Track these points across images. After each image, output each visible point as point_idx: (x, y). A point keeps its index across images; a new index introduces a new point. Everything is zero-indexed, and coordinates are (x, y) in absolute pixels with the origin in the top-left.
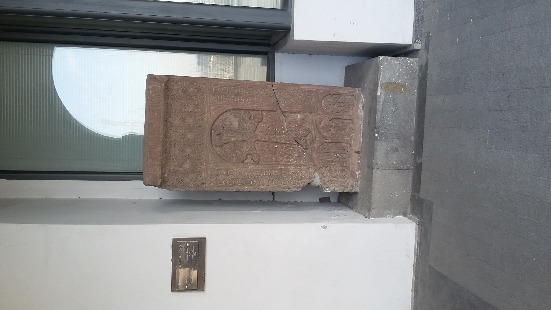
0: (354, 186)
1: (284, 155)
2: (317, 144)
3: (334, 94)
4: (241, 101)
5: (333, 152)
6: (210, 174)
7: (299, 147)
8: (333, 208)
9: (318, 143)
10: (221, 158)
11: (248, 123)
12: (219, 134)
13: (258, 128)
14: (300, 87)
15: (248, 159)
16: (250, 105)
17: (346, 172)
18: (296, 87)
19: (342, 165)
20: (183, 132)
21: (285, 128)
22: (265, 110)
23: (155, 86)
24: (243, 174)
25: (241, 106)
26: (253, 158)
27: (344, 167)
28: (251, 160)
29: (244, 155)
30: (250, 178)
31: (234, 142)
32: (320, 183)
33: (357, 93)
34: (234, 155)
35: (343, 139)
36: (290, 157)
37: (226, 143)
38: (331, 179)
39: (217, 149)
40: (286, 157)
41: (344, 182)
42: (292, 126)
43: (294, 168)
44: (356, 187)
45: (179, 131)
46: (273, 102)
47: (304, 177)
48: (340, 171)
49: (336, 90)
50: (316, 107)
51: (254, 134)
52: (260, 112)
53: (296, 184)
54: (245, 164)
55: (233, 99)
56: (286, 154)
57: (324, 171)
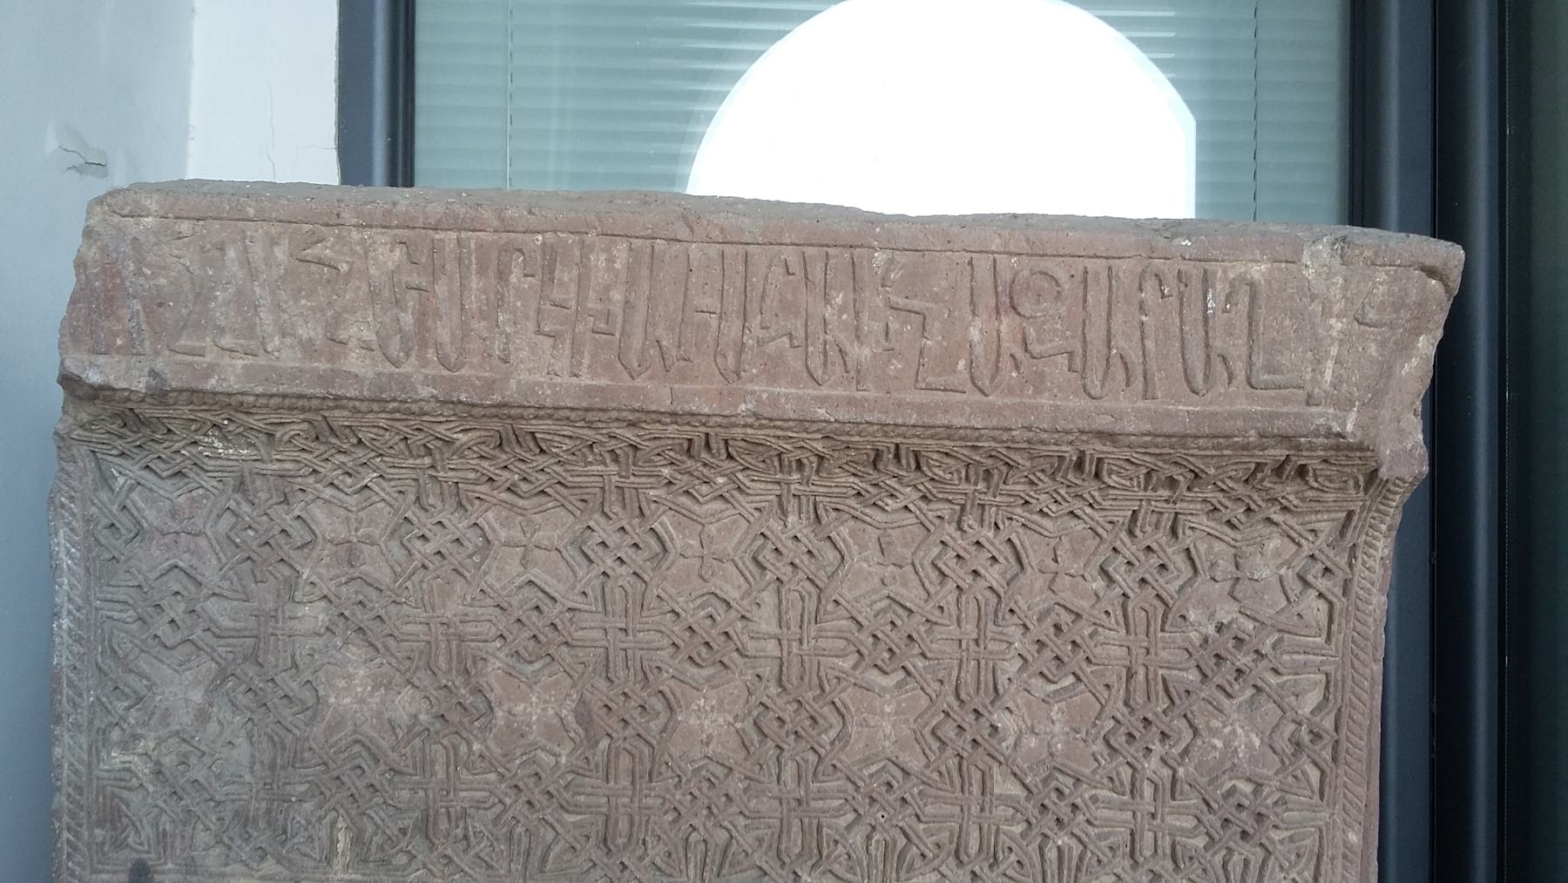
20: (751, 647)
23: (1337, 325)
45: (768, 597)
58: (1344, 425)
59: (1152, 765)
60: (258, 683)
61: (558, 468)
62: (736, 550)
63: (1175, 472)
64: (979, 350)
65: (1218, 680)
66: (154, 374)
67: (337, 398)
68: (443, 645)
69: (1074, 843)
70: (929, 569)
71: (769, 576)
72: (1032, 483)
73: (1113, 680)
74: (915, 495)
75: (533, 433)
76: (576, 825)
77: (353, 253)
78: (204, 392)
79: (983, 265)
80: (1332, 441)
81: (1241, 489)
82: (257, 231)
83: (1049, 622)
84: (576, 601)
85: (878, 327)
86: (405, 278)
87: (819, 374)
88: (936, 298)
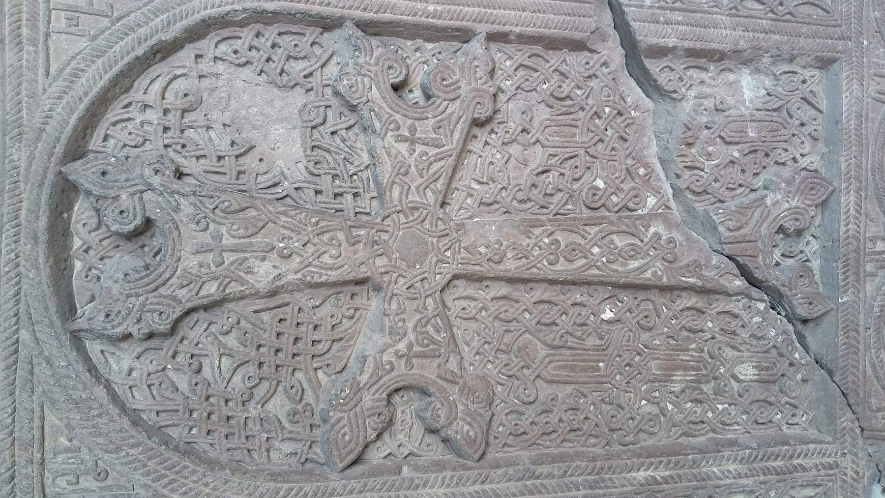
1: (667, 379)
2: (877, 280)
13: (466, 177)
15: (398, 426)
21: (658, 179)
22: (518, 30)
26: (443, 413)
28: (418, 430)
29: (368, 399)
31: (273, 294)
34: (279, 406)
36: (704, 387)
37: (206, 308)
40: (677, 388)
42: (709, 156)
43: (742, 468)
52: (476, 46)
54: (378, 472)
56: (676, 368)
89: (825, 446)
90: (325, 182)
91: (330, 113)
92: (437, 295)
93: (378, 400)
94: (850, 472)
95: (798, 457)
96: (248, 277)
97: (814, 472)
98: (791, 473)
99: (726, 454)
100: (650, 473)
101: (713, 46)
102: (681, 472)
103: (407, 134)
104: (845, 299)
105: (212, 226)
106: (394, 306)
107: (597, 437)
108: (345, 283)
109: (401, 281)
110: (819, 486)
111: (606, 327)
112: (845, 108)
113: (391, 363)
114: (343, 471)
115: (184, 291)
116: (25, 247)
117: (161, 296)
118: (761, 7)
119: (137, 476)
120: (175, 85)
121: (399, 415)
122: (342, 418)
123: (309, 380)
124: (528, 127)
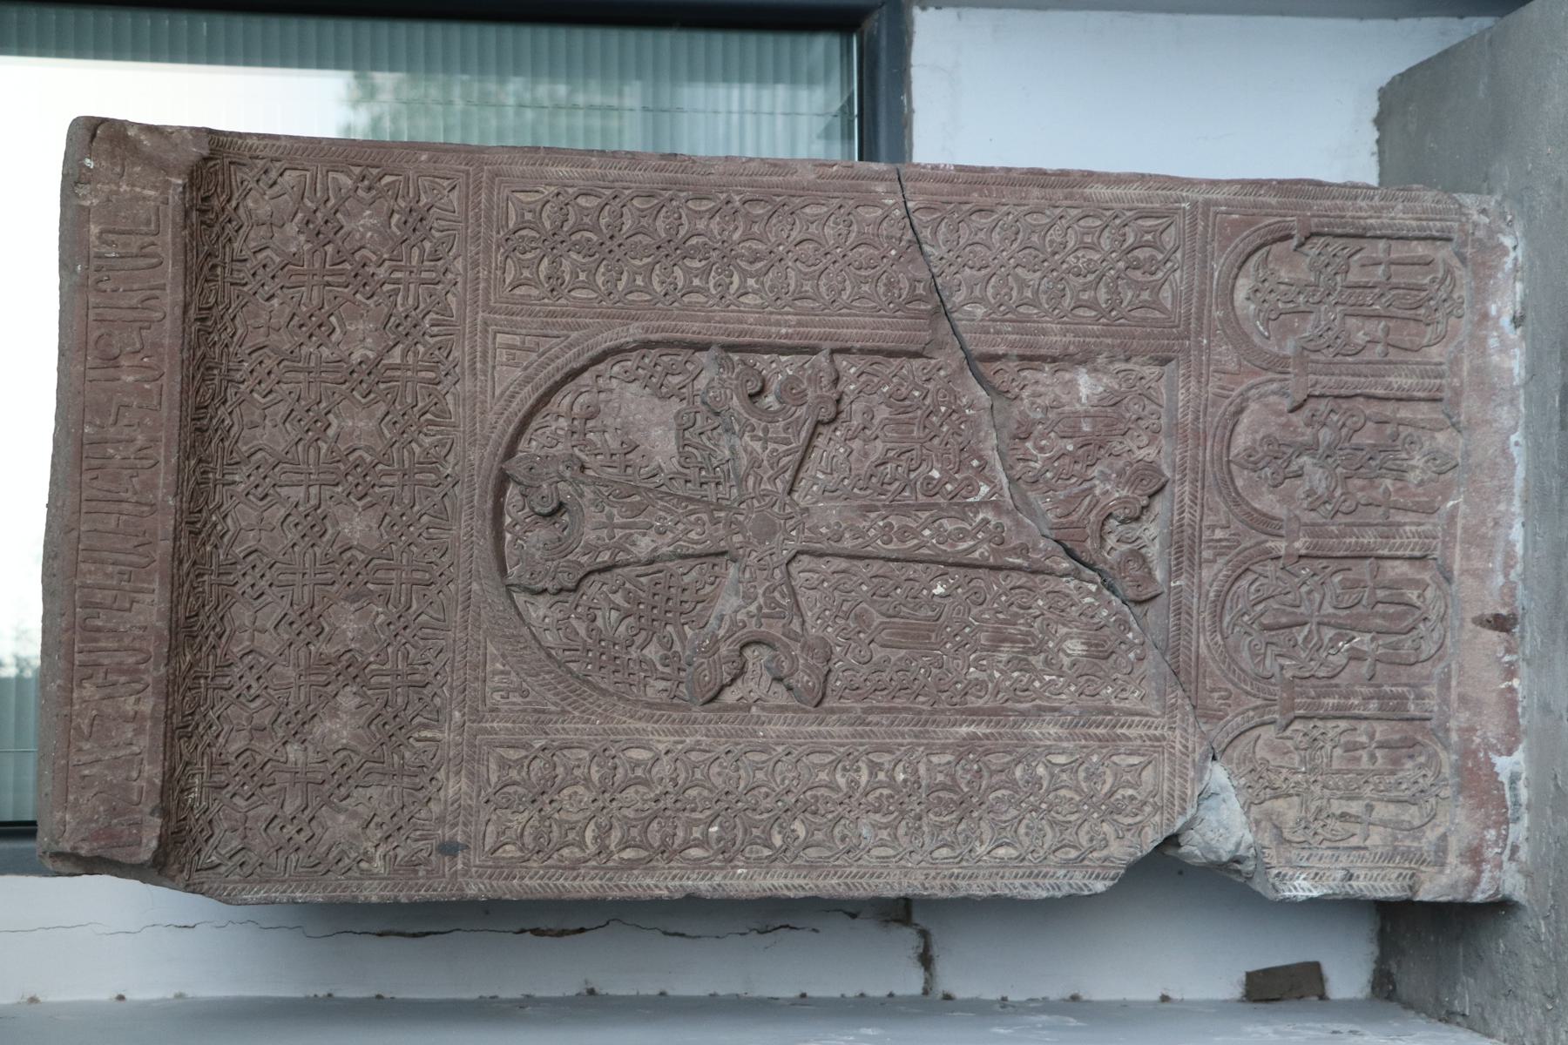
0: (1490, 853)
2: (1216, 567)
3: (1313, 235)
4: (697, 290)
5: (1328, 624)
6: (494, 779)
7: (1090, 593)
8: (1345, 1027)
9: (1221, 561)
10: (570, 672)
11: (747, 438)
12: (552, 514)
14: (1087, 191)
16: (751, 318)
17: (1422, 759)
18: (1060, 193)
19: (1393, 709)
20: (313, 502)
21: (993, 469)
22: (858, 345)
23: (124, 188)
24: (718, 781)
25: (696, 326)
27: (1405, 725)
28: (767, 677)
29: (724, 650)
30: (767, 803)
31: (651, 562)
32: (1249, 838)
33: (1476, 225)
34: (653, 652)
35: (1390, 529)
36: (1030, 658)
38: (1320, 810)
39: (538, 610)
40: (1004, 657)
41: (1415, 831)
42: (1042, 449)
43: (1063, 732)
44: (1500, 866)
45: (284, 491)
46: (905, 293)
47: (1130, 792)
48: (1379, 753)
49: (1328, 203)
50: (1199, 319)
51: (788, 510)
52: (822, 359)
53: (1084, 839)
54: (732, 708)
55: (639, 282)
57: (1273, 749)
58: (178, 185)
59: (382, 273)
60: (334, 783)
61: (207, 608)
62: (255, 510)
63: (206, 269)
64: (138, 377)
65: (331, 235)
66: (152, 814)
67: (166, 717)
68: (312, 678)
69: (428, 317)
70: (267, 399)
71: (271, 492)
72: (215, 344)
73: (331, 296)
74: (222, 408)
75: (187, 618)
76: (418, 602)
77: (87, 707)
78: (163, 787)
79: (92, 374)
80: (188, 190)
81: (217, 229)
82: (74, 759)
83: (298, 331)
84: (287, 601)
85: (127, 430)
86: (100, 681)
87: (152, 462)
88: (110, 400)
89: (1151, 719)
90: (692, 473)
91: (698, 416)
92: (783, 567)
93: (733, 651)
94: (1178, 746)
95: (1122, 726)
96: (633, 549)
97: (1139, 742)
98: (1114, 740)
99: (1048, 718)
100: (972, 729)
101: (1043, 352)
102: (1002, 731)
103: (761, 434)
104: (1178, 583)
105: (607, 508)
106: (747, 575)
107: (926, 695)
108: (707, 555)
109: (754, 554)
110: (1143, 755)
111: (939, 600)
112: (1180, 404)
113: (743, 622)
114: (704, 704)
115: (586, 557)
116: (477, 523)
117: (569, 561)
118: (1094, 313)
119: (549, 695)
120: (581, 399)
121: (750, 666)
122: (702, 663)
123: (678, 633)
124: (868, 425)
